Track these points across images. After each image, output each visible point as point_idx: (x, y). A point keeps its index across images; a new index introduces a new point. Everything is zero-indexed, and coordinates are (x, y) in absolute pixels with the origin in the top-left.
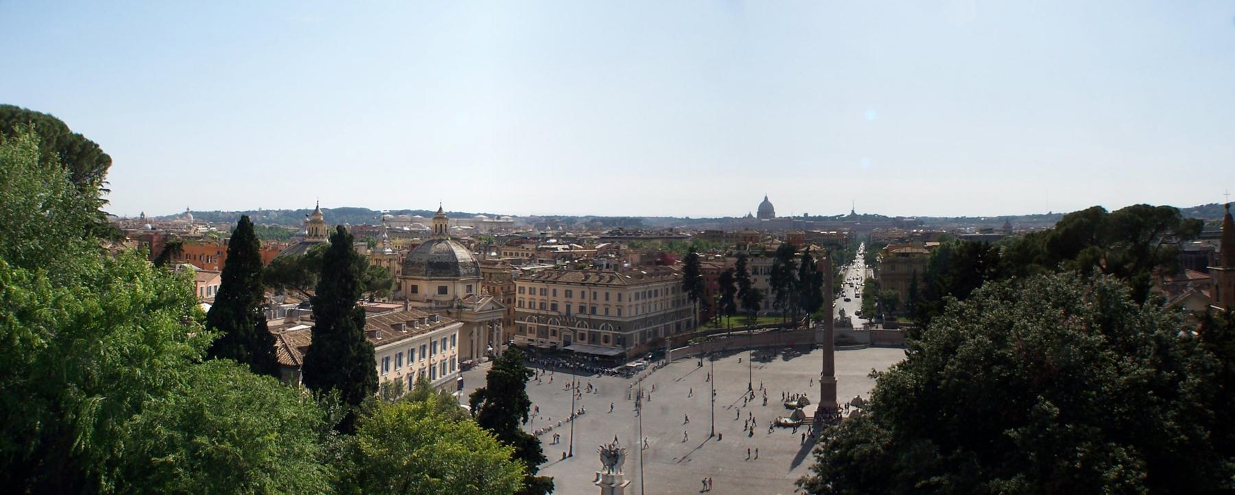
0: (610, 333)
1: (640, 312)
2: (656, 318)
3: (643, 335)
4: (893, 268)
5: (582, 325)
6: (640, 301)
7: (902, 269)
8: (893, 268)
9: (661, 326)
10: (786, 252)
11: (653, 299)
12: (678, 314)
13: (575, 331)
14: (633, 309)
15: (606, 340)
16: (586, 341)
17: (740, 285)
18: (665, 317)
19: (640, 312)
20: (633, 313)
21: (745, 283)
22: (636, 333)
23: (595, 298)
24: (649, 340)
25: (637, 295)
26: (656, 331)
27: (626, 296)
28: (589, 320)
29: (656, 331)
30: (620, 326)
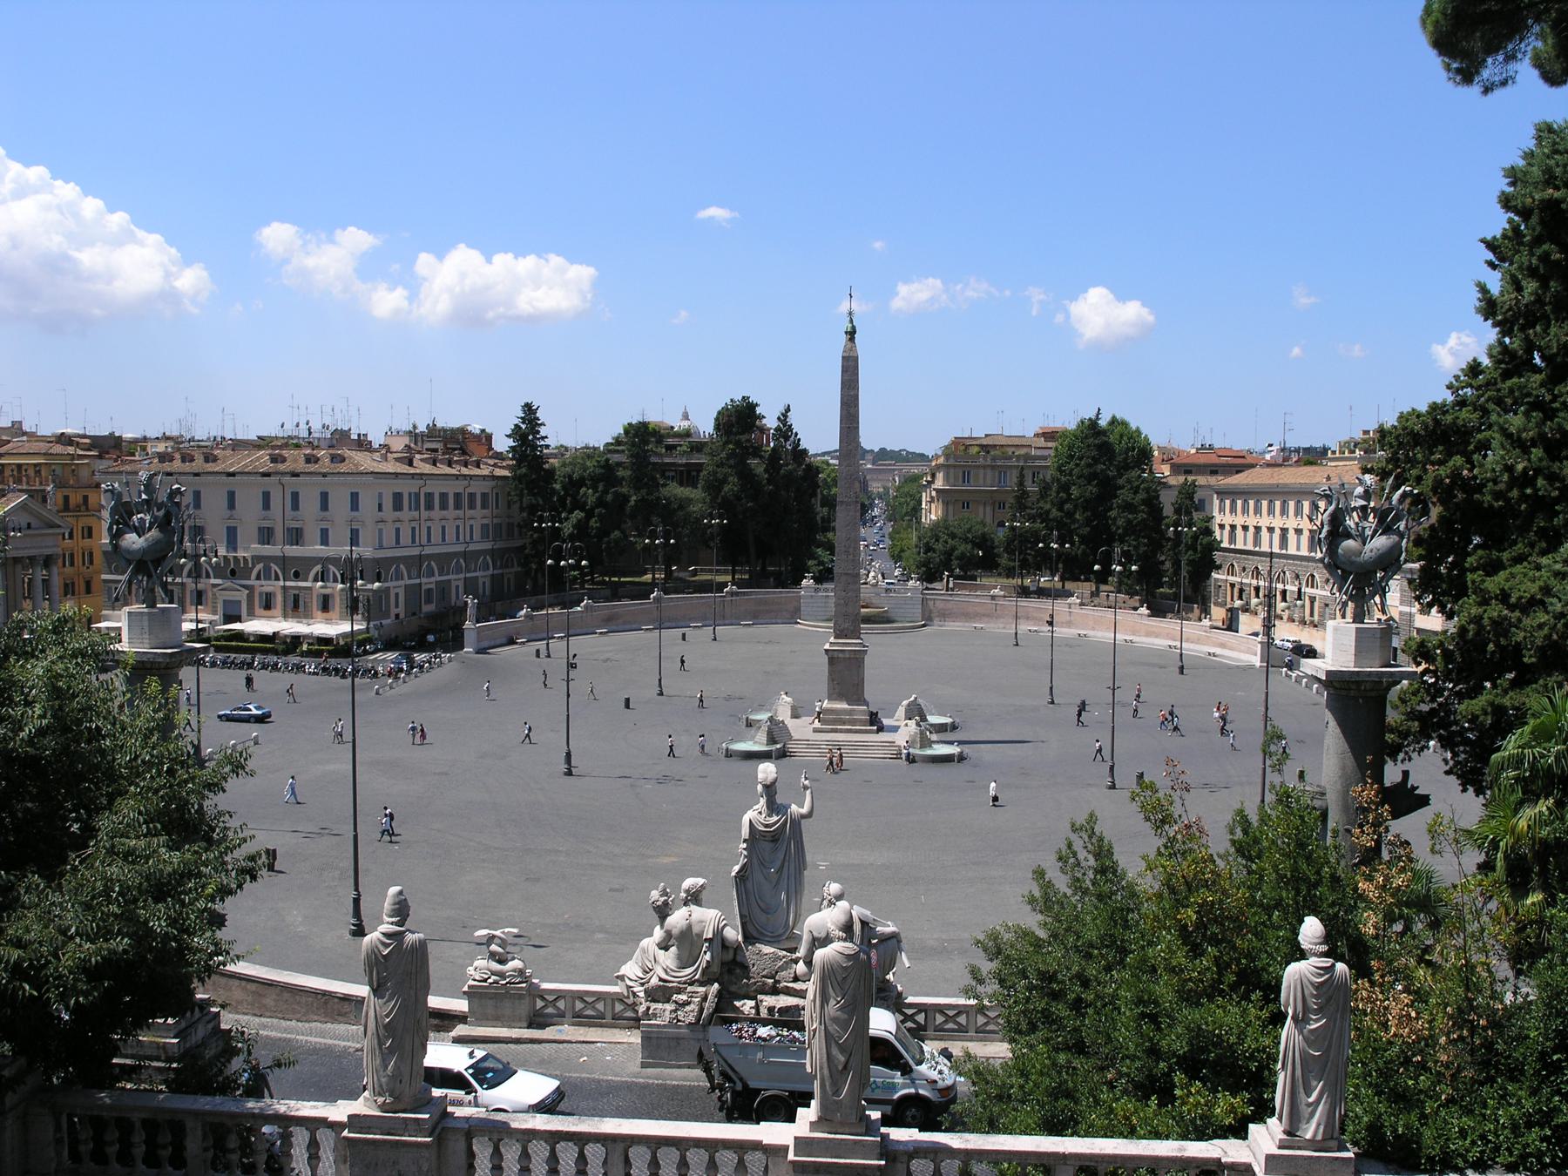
1: (405, 538)
2: (444, 561)
3: (413, 592)
4: (966, 478)
5: (266, 574)
6: (406, 514)
10: (740, 419)
11: (437, 513)
13: (250, 588)
15: (326, 605)
16: (278, 610)
19: (405, 538)
22: (397, 587)
23: (295, 507)
24: (428, 608)
25: (398, 498)
26: (444, 588)
27: (367, 503)
28: (284, 561)
30: (350, 571)
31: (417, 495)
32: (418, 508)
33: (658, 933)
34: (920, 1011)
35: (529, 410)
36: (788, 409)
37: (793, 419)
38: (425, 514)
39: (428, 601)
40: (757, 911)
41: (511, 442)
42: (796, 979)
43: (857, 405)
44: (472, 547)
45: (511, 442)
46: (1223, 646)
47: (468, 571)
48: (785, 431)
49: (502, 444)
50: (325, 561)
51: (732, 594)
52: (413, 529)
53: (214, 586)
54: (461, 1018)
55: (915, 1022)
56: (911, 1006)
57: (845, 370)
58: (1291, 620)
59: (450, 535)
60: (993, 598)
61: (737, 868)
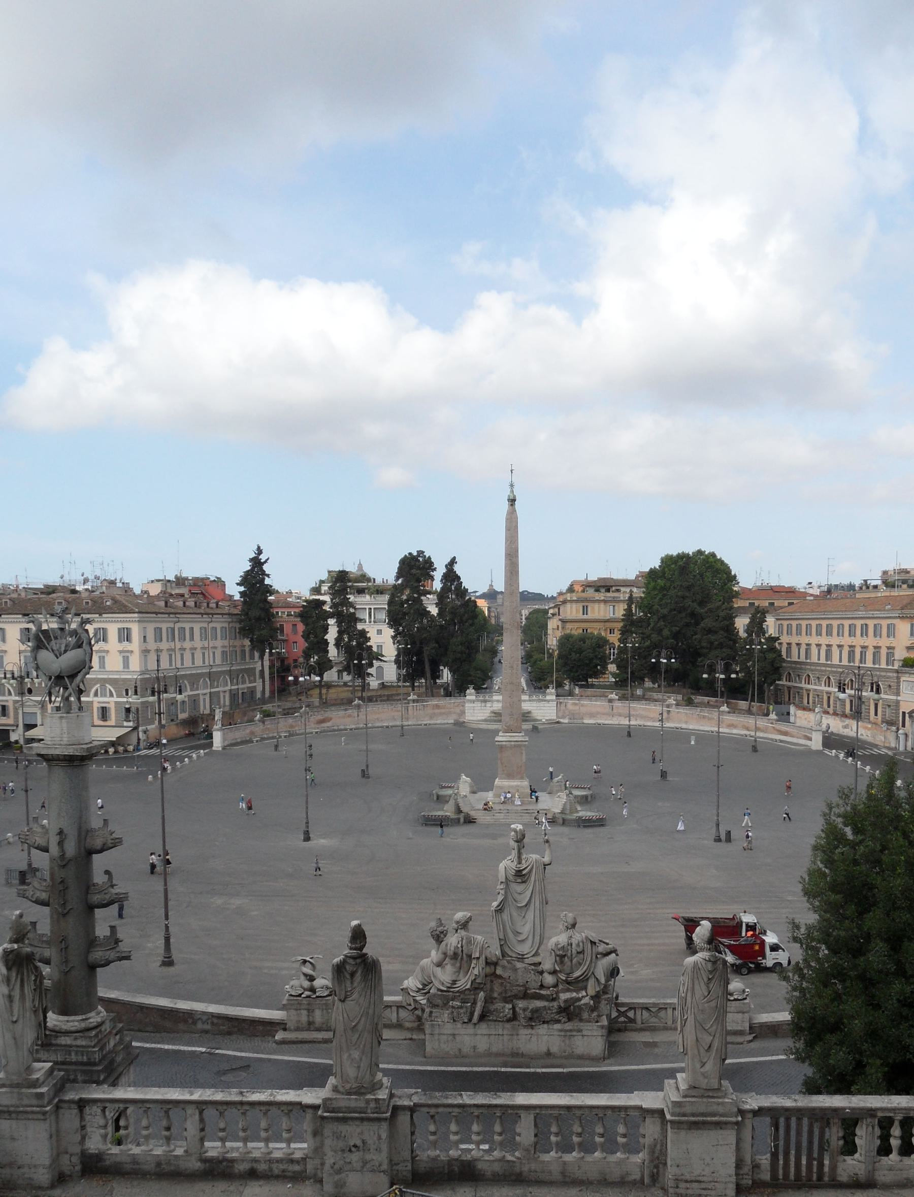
0: (112, 701)
2: (194, 679)
4: (585, 610)
6: (164, 645)
7: (599, 611)
8: (585, 610)
9: (203, 692)
10: (415, 568)
11: (187, 644)
12: (233, 675)
14: (153, 657)
17: (339, 623)
18: (212, 677)
20: (153, 666)
21: (348, 621)
24: (182, 716)
26: (194, 701)
29: (194, 701)
31: (173, 630)
32: (173, 639)
33: (435, 955)
34: (631, 1009)
35: (257, 563)
36: (453, 561)
37: (457, 568)
38: (178, 645)
39: (183, 711)
40: (511, 935)
41: (242, 589)
42: (542, 986)
43: (517, 556)
44: (214, 670)
45: (242, 589)
46: (786, 734)
47: (212, 686)
48: (451, 576)
49: (234, 590)
50: (104, 682)
51: (414, 701)
52: (170, 656)
53: (15, 702)
54: (282, 1025)
55: (627, 1017)
56: (623, 1005)
57: (508, 529)
58: (835, 714)
59: (199, 662)
60: (610, 701)
61: (495, 904)
